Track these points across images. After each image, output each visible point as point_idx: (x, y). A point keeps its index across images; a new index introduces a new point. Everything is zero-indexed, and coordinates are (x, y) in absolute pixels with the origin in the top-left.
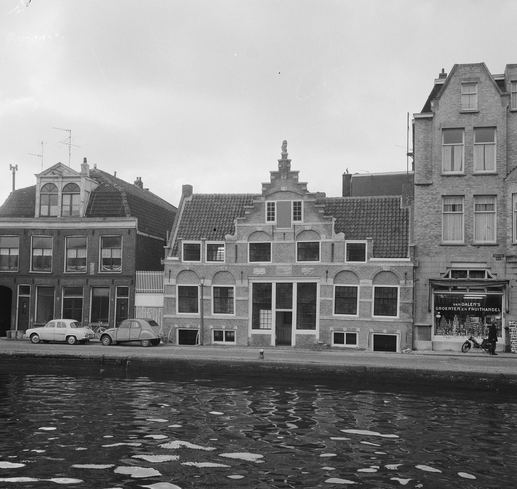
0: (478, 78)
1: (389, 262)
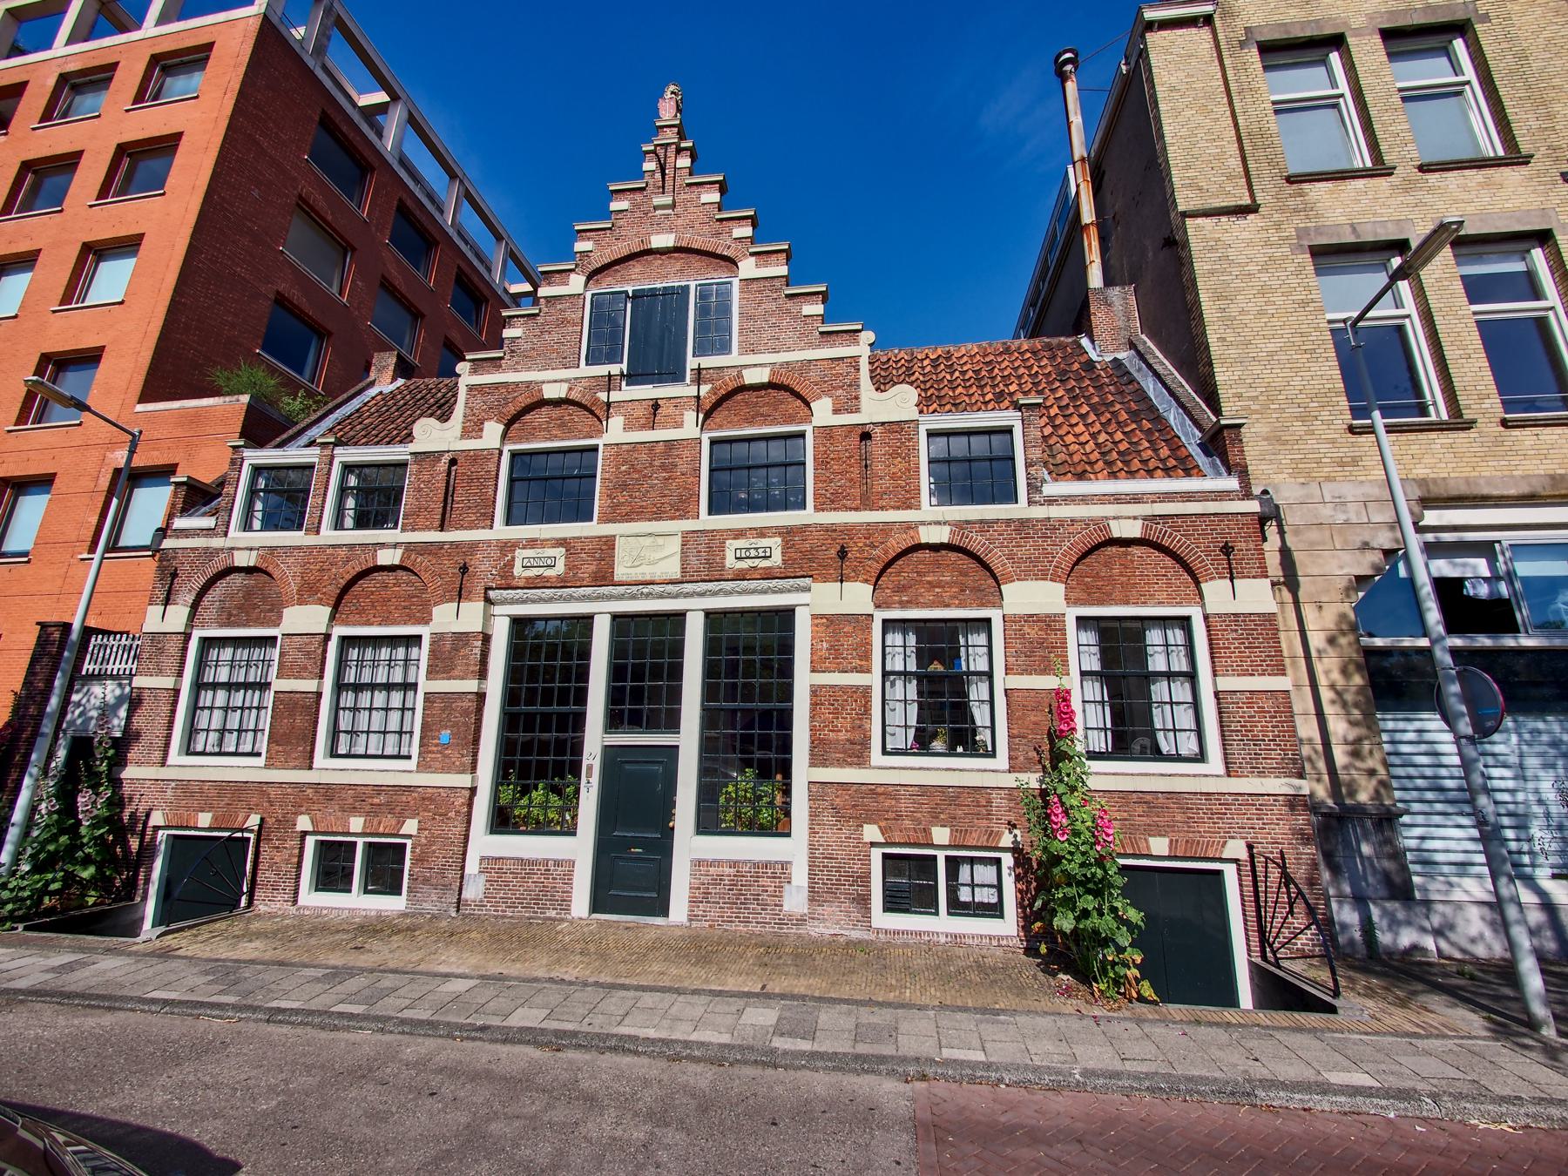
1: (1136, 499)
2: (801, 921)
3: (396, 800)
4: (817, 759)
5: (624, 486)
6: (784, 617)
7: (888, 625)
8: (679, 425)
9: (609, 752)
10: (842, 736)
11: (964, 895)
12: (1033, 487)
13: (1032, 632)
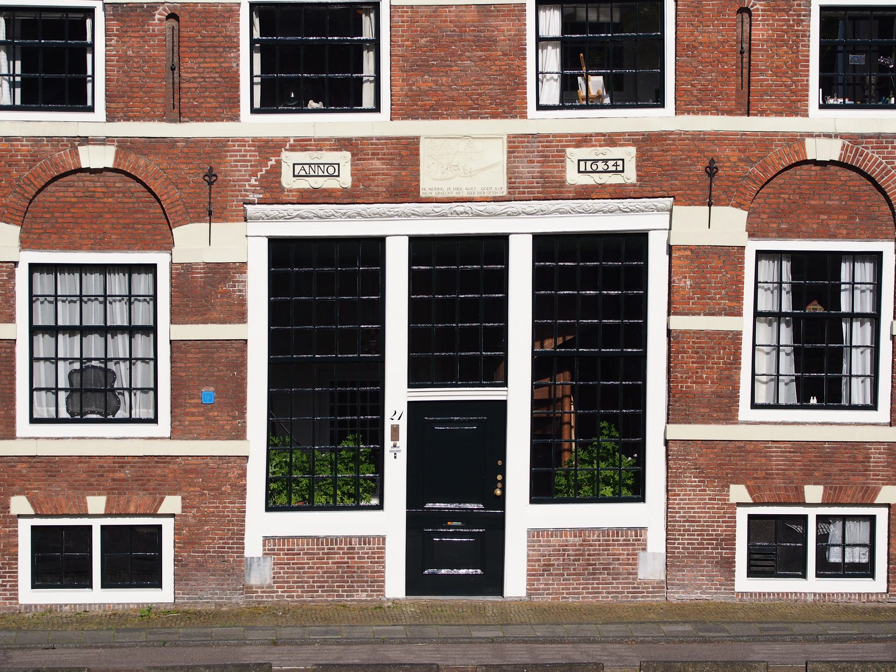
2: (659, 587)
3: (143, 477)
6: (636, 243)
7: (761, 255)
10: (708, 388)
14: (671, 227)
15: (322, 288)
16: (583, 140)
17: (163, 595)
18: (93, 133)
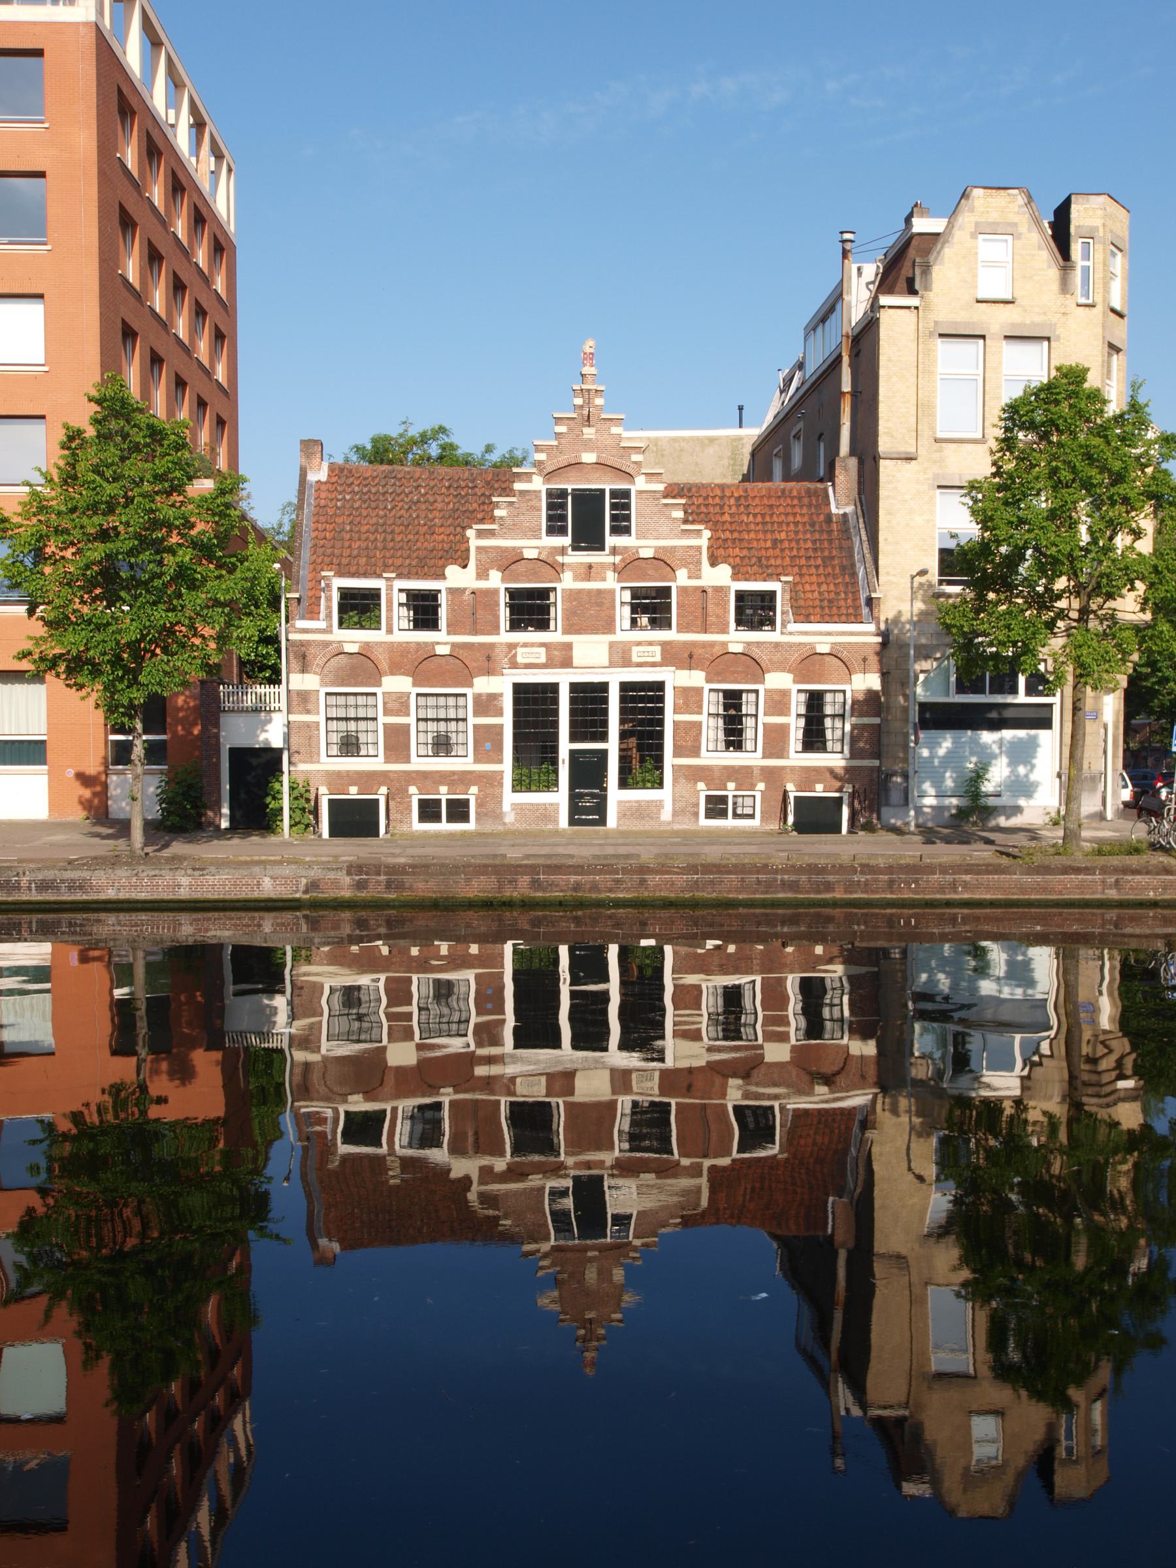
0: (1015, 225)
1: (829, 634)
2: (669, 823)
4: (676, 754)
5: (574, 614)
6: (660, 686)
8: (604, 580)
9: (573, 753)
11: (739, 811)
12: (784, 625)
13: (777, 698)
14: (674, 679)
15: (534, 703)
16: (639, 644)
17: (471, 826)
18: (441, 640)
